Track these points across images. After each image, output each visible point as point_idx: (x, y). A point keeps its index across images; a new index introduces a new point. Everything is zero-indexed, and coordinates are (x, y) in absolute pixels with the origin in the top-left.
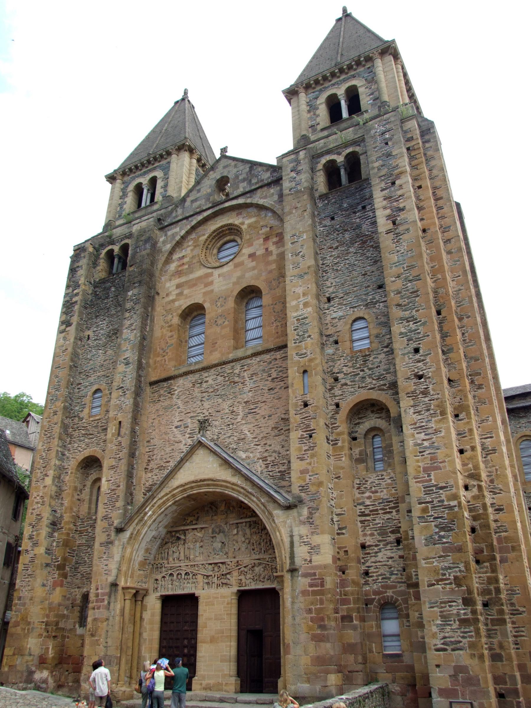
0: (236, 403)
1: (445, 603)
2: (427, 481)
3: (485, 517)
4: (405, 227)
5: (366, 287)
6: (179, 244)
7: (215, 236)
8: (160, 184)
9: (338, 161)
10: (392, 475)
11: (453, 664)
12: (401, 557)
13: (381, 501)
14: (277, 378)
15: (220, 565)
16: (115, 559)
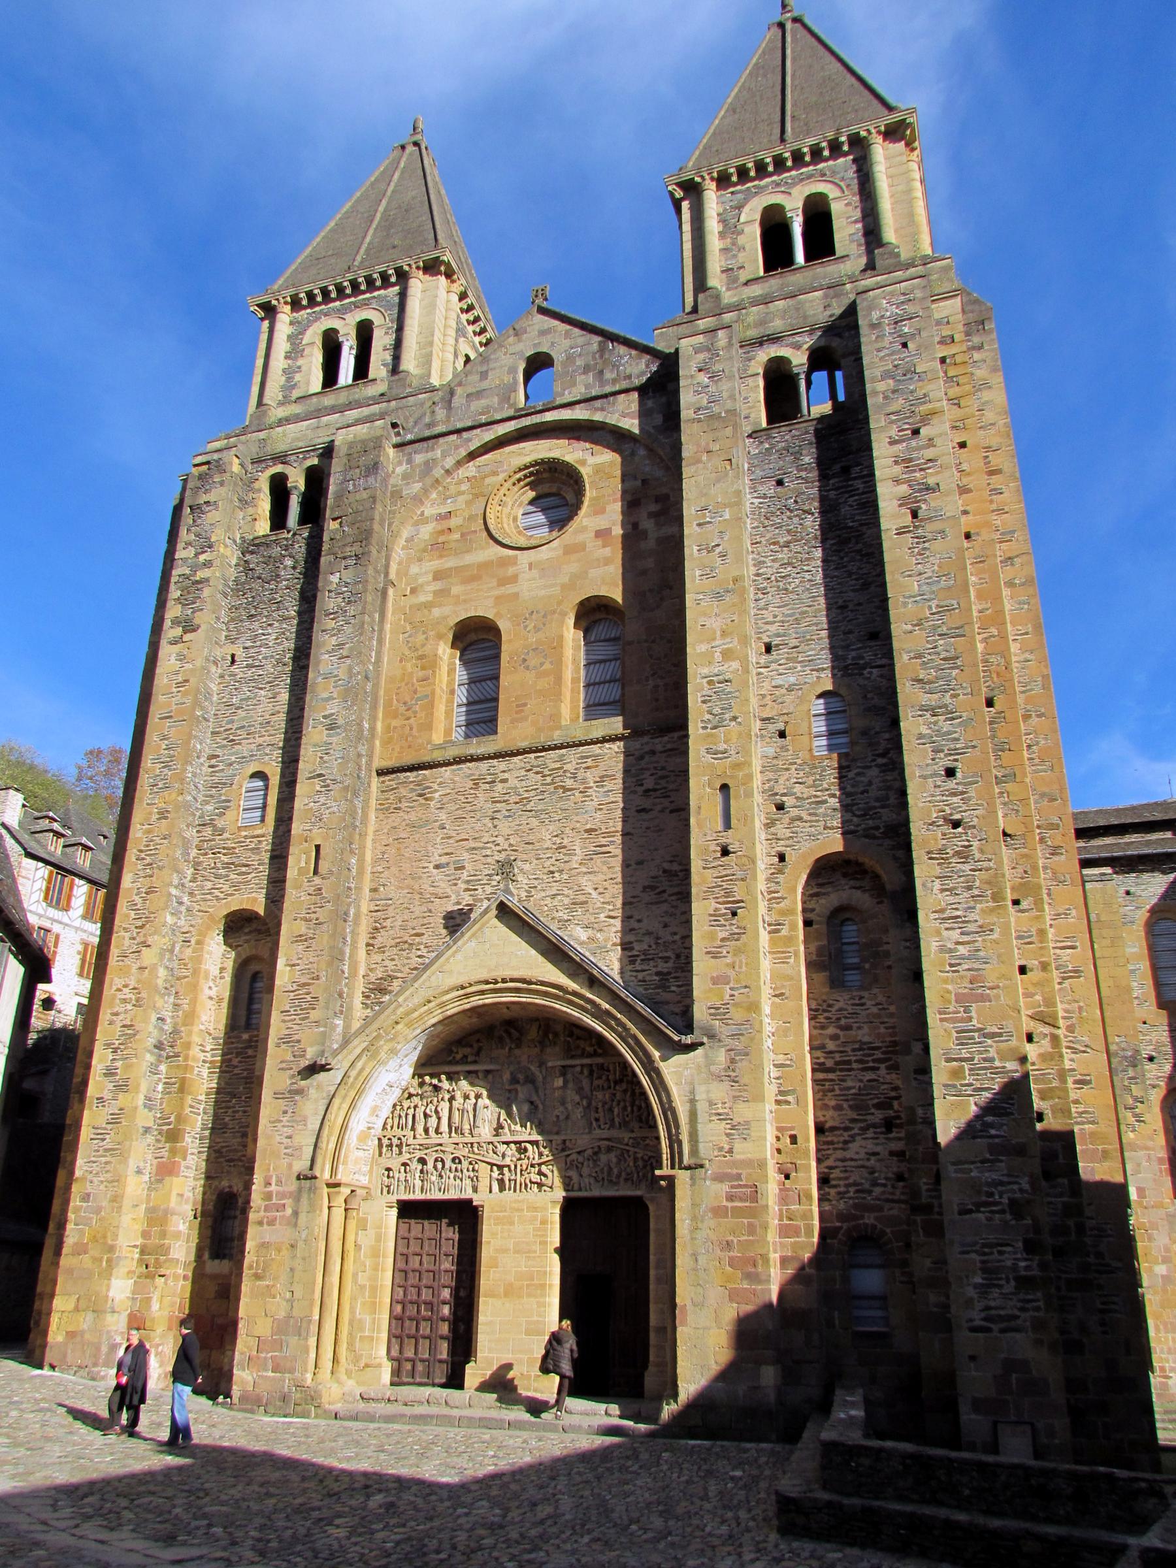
0: (567, 830)
1: (991, 1246)
2: (962, 1020)
3: (1062, 1094)
4: (937, 526)
5: (845, 633)
7: (519, 480)
8: (381, 341)
9: (795, 362)
10: (881, 998)
11: (1003, 1356)
12: (892, 1153)
13: (857, 1046)
14: (655, 790)
15: (528, 1145)
16: (310, 1126)
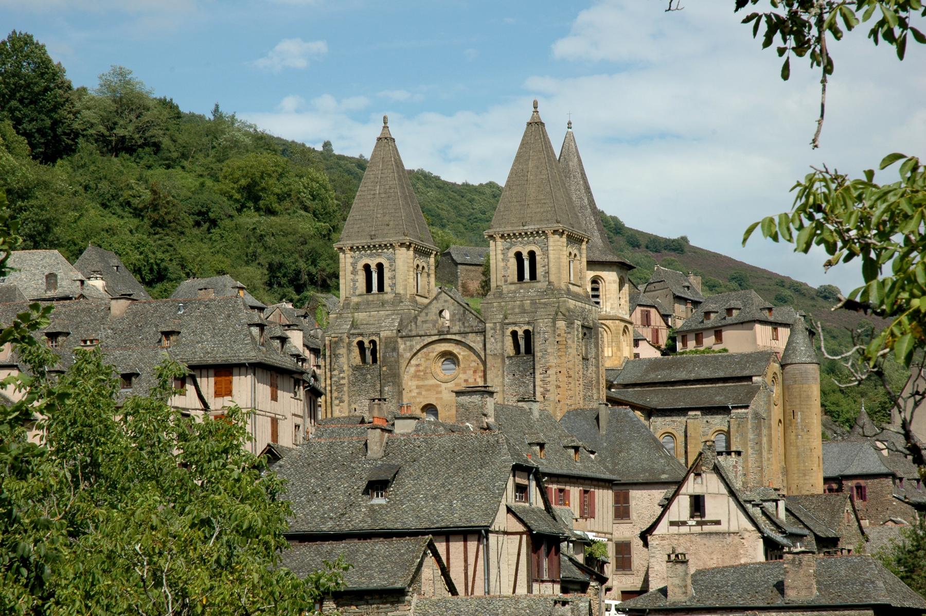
8: (387, 274)
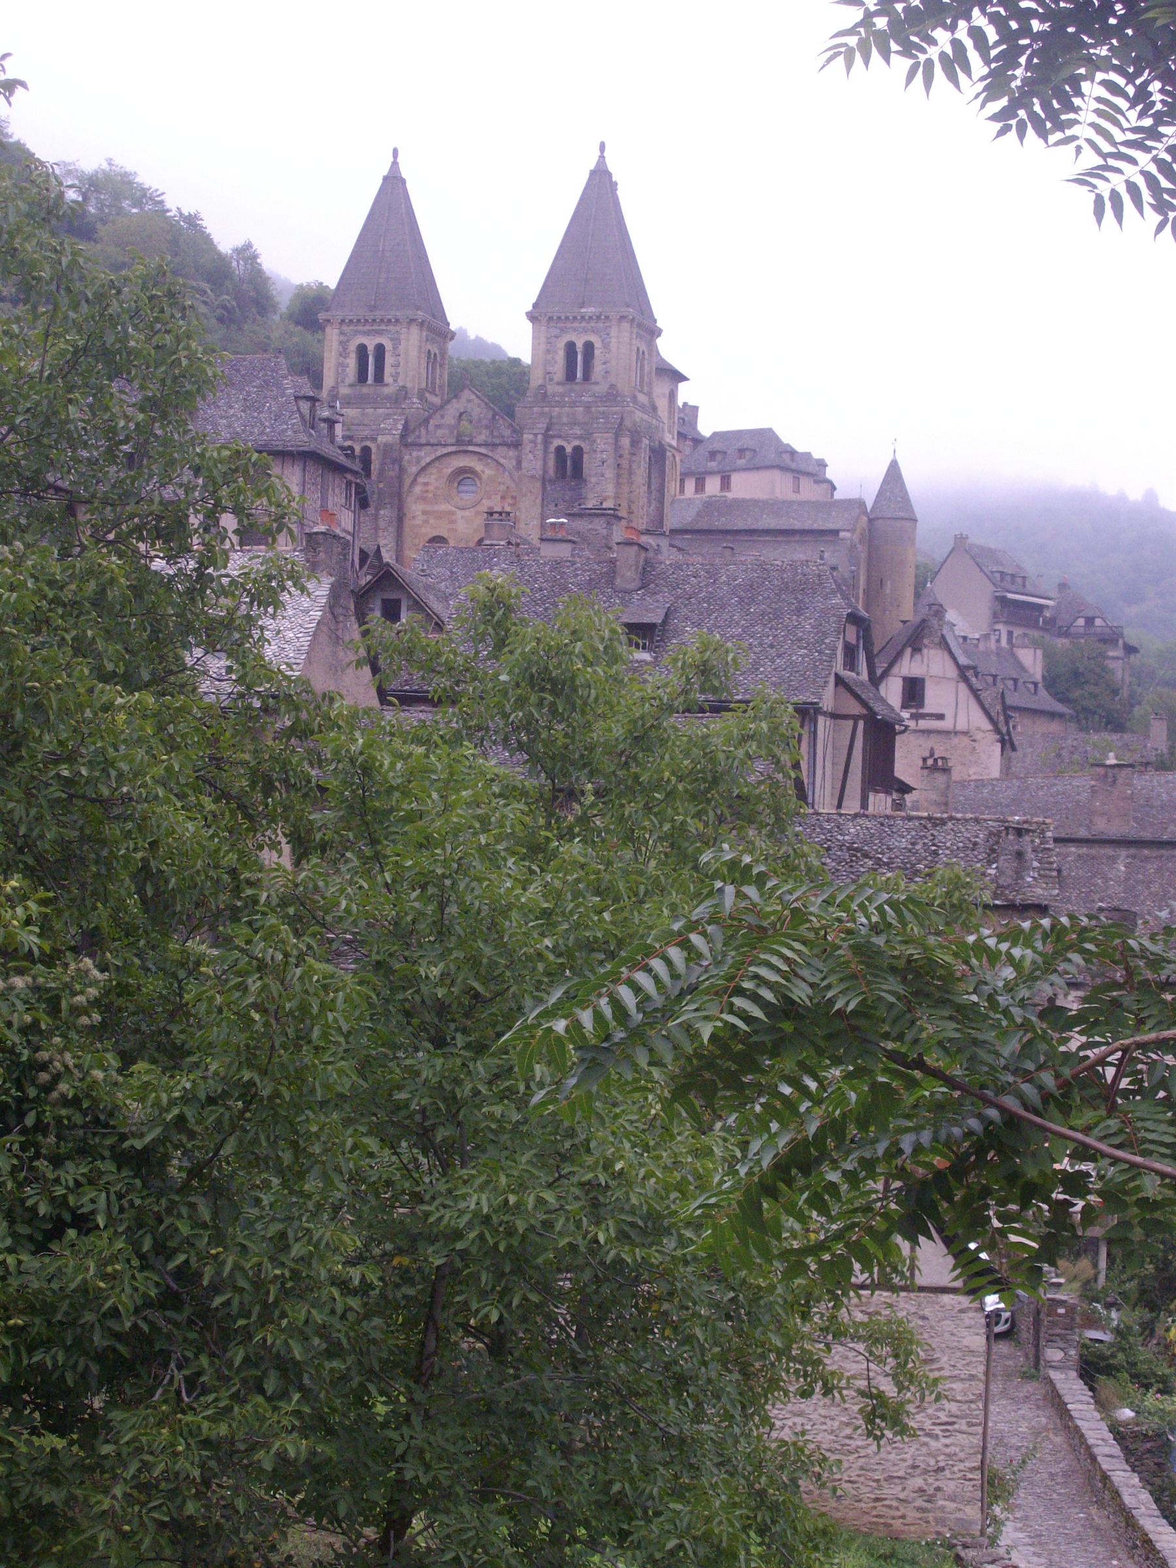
6: (423, 469)
8: (389, 360)
